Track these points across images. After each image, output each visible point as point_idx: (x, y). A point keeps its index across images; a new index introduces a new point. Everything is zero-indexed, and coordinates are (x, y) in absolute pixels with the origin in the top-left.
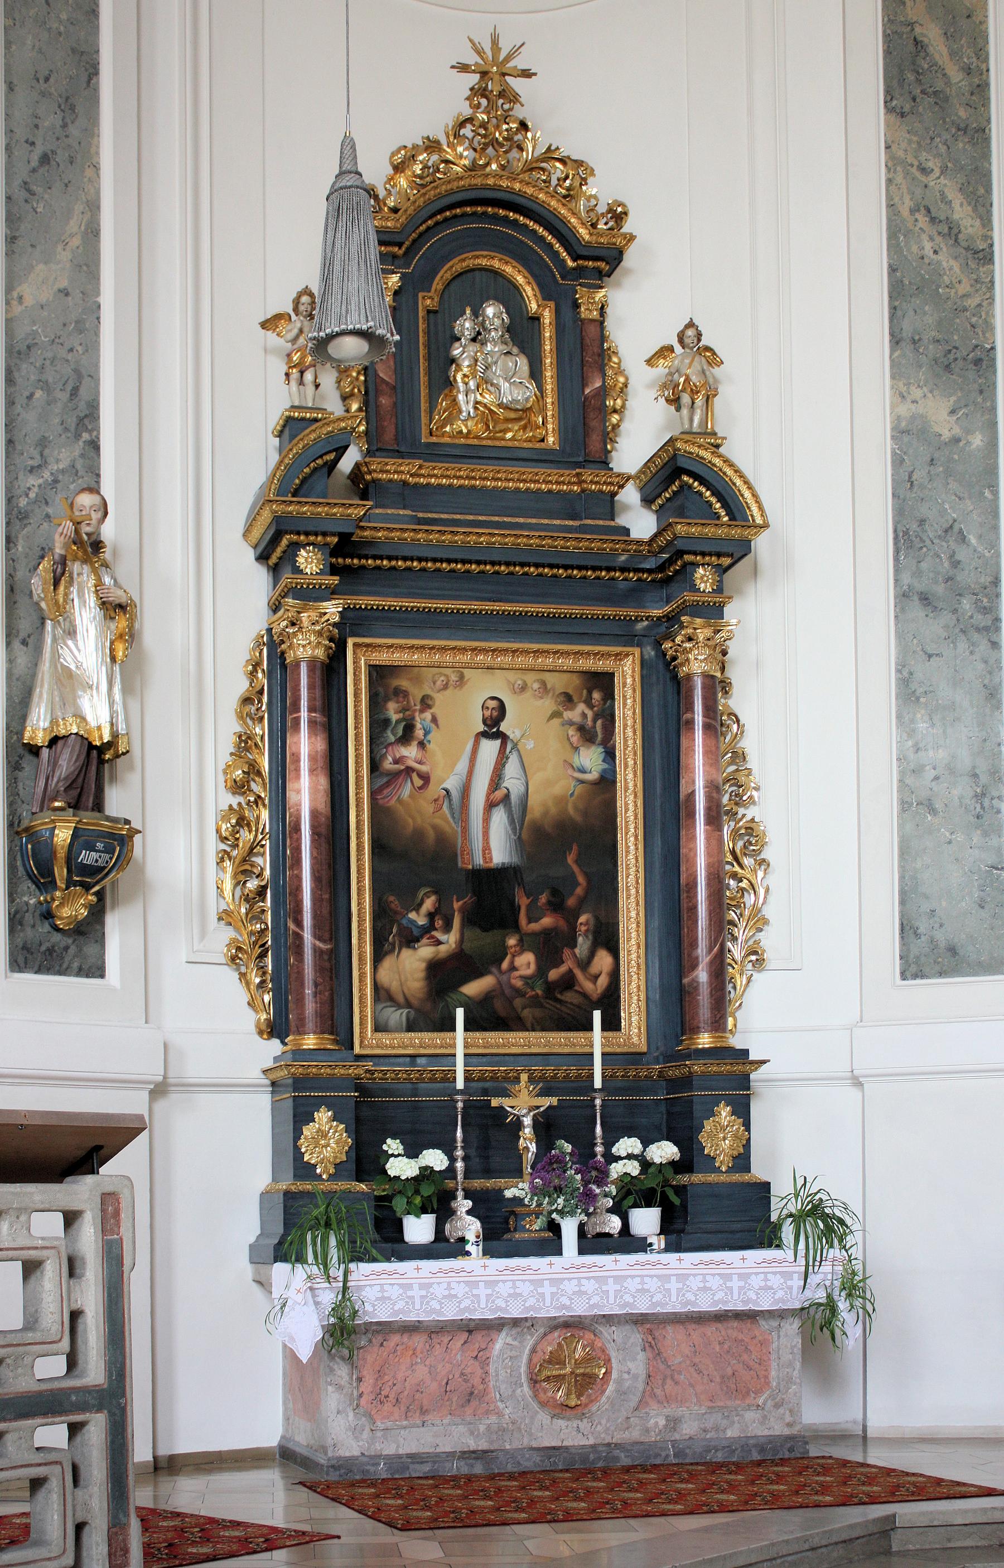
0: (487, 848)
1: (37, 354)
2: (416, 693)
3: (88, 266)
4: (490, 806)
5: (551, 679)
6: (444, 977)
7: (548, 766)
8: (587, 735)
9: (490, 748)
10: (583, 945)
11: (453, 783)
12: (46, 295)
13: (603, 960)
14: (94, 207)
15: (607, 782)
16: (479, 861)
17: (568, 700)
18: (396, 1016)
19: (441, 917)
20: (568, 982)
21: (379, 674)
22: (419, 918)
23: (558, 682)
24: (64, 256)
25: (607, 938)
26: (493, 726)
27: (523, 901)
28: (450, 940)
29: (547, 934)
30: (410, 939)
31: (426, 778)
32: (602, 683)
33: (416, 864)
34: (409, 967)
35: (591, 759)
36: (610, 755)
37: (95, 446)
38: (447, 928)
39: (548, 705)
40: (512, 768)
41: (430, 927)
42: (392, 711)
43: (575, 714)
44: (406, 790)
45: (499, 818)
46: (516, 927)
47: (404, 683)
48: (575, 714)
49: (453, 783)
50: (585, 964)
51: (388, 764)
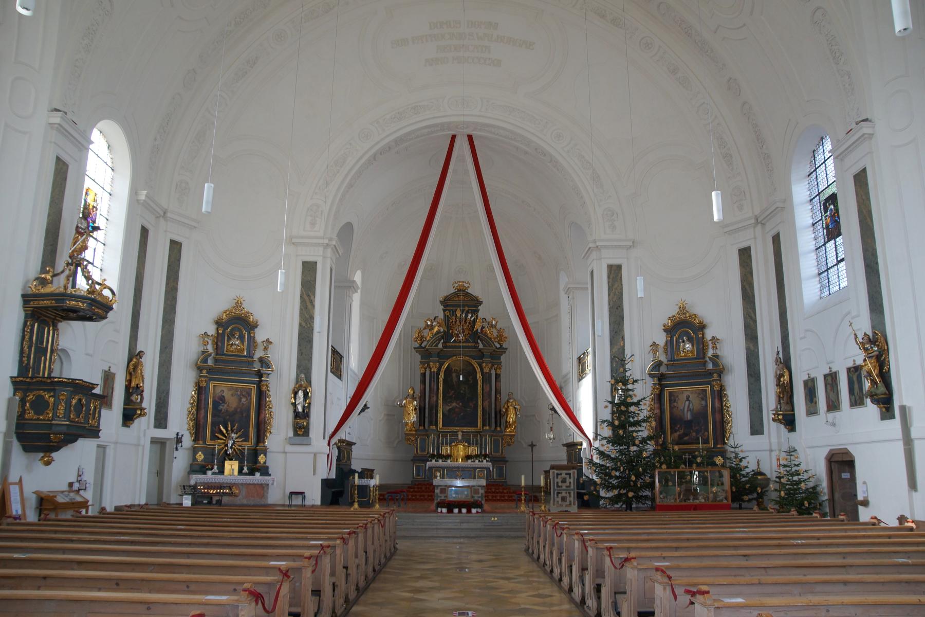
6: (681, 437)
7: (696, 404)
8: (702, 399)
15: (706, 406)
21: (670, 393)
26: (688, 399)
30: (676, 431)
35: (703, 402)
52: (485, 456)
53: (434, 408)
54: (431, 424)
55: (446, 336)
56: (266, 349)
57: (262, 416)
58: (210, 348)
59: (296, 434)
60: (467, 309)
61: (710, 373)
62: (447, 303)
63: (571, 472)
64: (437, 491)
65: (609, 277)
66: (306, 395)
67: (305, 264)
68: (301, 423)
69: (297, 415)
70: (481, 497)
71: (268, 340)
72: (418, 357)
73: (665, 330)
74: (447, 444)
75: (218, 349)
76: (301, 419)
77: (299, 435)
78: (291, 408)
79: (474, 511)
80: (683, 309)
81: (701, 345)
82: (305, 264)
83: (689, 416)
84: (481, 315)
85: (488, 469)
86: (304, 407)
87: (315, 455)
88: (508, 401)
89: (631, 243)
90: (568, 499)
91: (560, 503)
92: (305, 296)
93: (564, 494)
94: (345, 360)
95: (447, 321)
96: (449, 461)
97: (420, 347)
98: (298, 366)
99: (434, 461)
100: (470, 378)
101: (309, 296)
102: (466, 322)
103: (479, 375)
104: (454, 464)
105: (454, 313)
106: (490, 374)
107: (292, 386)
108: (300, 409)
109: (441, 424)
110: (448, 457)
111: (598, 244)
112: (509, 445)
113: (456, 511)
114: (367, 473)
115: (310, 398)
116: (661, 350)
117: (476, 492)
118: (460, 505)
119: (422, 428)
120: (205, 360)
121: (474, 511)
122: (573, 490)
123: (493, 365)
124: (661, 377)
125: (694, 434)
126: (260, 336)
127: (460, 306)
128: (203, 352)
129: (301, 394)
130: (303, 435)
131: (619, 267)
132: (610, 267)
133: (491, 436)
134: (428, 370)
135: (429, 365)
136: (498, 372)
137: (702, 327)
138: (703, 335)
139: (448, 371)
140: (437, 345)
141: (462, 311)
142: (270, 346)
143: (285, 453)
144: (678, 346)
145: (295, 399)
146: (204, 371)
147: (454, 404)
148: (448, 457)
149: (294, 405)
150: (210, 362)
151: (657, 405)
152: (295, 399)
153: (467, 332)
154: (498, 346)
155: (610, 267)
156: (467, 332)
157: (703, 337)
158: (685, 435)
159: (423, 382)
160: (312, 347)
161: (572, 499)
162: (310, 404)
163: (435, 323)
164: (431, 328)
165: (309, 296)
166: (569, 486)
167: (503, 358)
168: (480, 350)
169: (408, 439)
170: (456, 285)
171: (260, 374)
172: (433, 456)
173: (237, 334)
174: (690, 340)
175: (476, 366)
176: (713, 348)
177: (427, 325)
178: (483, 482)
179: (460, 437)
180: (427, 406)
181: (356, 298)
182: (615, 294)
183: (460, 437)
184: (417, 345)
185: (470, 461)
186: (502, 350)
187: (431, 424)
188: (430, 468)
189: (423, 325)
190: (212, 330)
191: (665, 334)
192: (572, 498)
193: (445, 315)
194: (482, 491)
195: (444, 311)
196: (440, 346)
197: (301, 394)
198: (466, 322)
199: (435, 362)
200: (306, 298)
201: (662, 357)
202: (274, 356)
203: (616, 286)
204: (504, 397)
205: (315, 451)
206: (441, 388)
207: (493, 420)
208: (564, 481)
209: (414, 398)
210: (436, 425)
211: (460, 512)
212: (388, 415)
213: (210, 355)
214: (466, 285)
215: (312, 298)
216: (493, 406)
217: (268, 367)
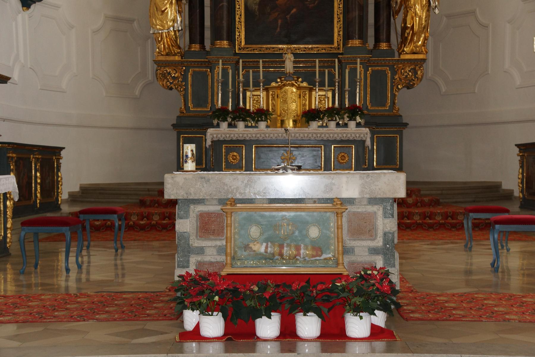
52: (353, 111)
54: (217, 36)
70: (385, 251)
74: (256, 85)
79: (357, 326)
85: (360, 144)
96: (262, 125)
99: (224, 125)
104: (277, 133)
109: (241, 34)
110: (261, 114)
112: (409, 87)
113: (268, 327)
117: (363, 228)
118: (289, 295)
119: (196, 47)
121: (357, 326)
133: (366, 65)
148: (261, 114)
169: (164, 76)
172: (222, 114)
179: (289, 66)
183: (289, 66)
185: (314, 125)
187: (217, 36)
188: (217, 143)
194: (387, 224)
207: (371, 32)
210: (231, 39)
211: (288, 334)
212: (116, 19)
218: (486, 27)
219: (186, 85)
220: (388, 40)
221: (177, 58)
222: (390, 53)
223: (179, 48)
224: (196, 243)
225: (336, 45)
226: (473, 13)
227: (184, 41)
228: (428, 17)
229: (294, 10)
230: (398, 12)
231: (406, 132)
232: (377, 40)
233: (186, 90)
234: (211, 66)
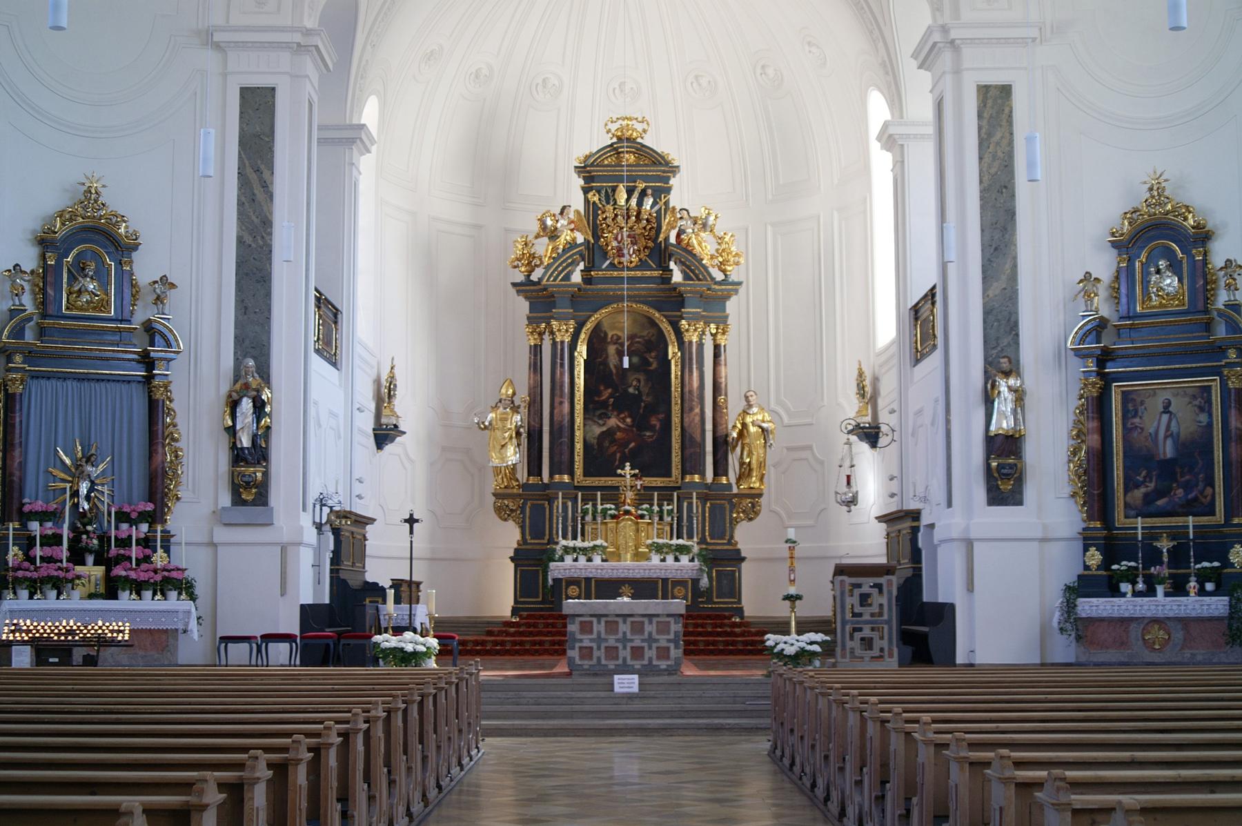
0: (1165, 453)
1: (994, 312)
2: (1139, 400)
3: (1013, 278)
4: (1166, 437)
5: (1188, 391)
6: (1148, 499)
7: (1186, 420)
8: (1201, 409)
9: (1165, 417)
10: (1201, 485)
11: (1152, 430)
12: (997, 292)
13: (1209, 490)
14: (1015, 258)
15: (1210, 425)
16: (1162, 457)
17: (1194, 397)
18: (1133, 513)
19: (1148, 477)
20: (1196, 499)
22: (1140, 478)
23: (1190, 391)
24: (1004, 277)
25: (1210, 482)
26: (1166, 409)
27: (1178, 470)
28: (1152, 485)
29: (1188, 482)
30: (1137, 486)
31: (1142, 429)
32: (1207, 389)
33: (1138, 459)
34: (1139, 493)
35: (1203, 418)
36: (1210, 415)
37: (1017, 335)
38: (1151, 481)
39: (1187, 399)
40: (1173, 423)
41: (1144, 481)
42: (1130, 407)
43: (1197, 403)
44: (1135, 434)
45: (1169, 442)
46: (1176, 481)
47: (1134, 396)
48: (1197, 403)
49: (1152, 430)
50: (1202, 492)
51: (1129, 425)
53: (562, 432)
55: (593, 253)
56: (159, 299)
57: (159, 458)
58: (28, 302)
59: (238, 501)
60: (642, 185)
61: (1219, 350)
62: (590, 172)
63: (882, 580)
64: (573, 628)
65: (980, 116)
66: (259, 407)
67: (247, 94)
68: (249, 475)
69: (238, 457)
71: (164, 279)
72: (523, 306)
73: (1114, 244)
75: (44, 305)
76: (248, 464)
77: (244, 503)
78: (225, 441)
80: (1157, 192)
81: (1202, 281)
82: (247, 94)
83: (1168, 450)
84: (675, 199)
86: (254, 438)
87: (284, 549)
88: (745, 413)
89: (1034, 33)
90: (877, 644)
91: (858, 652)
92: (249, 171)
93: (867, 632)
94: (344, 318)
95: (592, 218)
97: (528, 282)
98: (239, 340)
100: (651, 357)
101: (258, 170)
102: (638, 216)
103: (673, 350)
105: (610, 196)
106: (700, 345)
107: (225, 388)
108: (245, 442)
111: (953, 34)
114: (407, 590)
115: (270, 415)
116: (1103, 291)
119: (532, 480)
120: (18, 332)
122: (888, 622)
123: (707, 324)
124: (1104, 358)
125: (1180, 492)
126: (145, 269)
127: (620, 179)
128: (13, 313)
129: (246, 405)
130: (254, 503)
131: (1006, 91)
132: (984, 91)
133: (703, 499)
134: (547, 337)
135: (548, 324)
136: (722, 340)
137: (1203, 236)
138: (1205, 254)
139: (597, 343)
140: (567, 278)
141: (630, 192)
142: (172, 293)
143: (213, 545)
144: (1146, 283)
145: (233, 416)
146: (18, 358)
147: (613, 422)
149: (232, 431)
150: (29, 336)
151: (1094, 424)
152: (233, 416)
153: (643, 242)
154: (719, 276)
155: (984, 91)
156: (643, 242)
157: (1205, 262)
158: (1159, 493)
159: (536, 367)
160: (268, 295)
161: (885, 644)
162: (268, 428)
163: (563, 222)
164: (553, 235)
165: (258, 170)
166: (881, 614)
167: (731, 306)
168: (674, 288)
170: (614, 127)
171: (148, 362)
173: (91, 268)
174: (1175, 267)
175: (666, 327)
176: (1228, 286)
177: (544, 226)
178: (678, 605)
180: (546, 428)
181: (366, 165)
182: (994, 157)
184: (520, 278)
186: (730, 287)
189: (536, 227)
190: (29, 259)
191: (1115, 252)
192: (886, 640)
193: (587, 201)
194: (676, 627)
195: (586, 191)
196: (577, 277)
197: (246, 405)
198: (638, 216)
199: (562, 318)
200: (253, 177)
201: (1105, 311)
202: (177, 317)
203: (998, 135)
204: (733, 406)
205: (285, 539)
206: (580, 381)
208: (864, 599)
209: (516, 409)
213: (29, 319)
214: (639, 127)
215: (266, 174)
216: (709, 426)
217: (169, 346)
218: (822, 463)
219: (524, 518)
220: (726, 474)
221: (515, 491)
222: (729, 486)
223: (517, 480)
224: (579, 636)
225: (673, 478)
226: (809, 448)
227: (522, 475)
228: (765, 453)
229: (632, 445)
230: (734, 448)
231: (744, 565)
232: (716, 474)
233: (524, 521)
234: (551, 500)
